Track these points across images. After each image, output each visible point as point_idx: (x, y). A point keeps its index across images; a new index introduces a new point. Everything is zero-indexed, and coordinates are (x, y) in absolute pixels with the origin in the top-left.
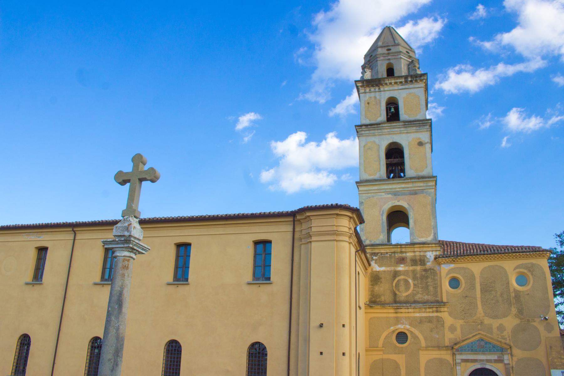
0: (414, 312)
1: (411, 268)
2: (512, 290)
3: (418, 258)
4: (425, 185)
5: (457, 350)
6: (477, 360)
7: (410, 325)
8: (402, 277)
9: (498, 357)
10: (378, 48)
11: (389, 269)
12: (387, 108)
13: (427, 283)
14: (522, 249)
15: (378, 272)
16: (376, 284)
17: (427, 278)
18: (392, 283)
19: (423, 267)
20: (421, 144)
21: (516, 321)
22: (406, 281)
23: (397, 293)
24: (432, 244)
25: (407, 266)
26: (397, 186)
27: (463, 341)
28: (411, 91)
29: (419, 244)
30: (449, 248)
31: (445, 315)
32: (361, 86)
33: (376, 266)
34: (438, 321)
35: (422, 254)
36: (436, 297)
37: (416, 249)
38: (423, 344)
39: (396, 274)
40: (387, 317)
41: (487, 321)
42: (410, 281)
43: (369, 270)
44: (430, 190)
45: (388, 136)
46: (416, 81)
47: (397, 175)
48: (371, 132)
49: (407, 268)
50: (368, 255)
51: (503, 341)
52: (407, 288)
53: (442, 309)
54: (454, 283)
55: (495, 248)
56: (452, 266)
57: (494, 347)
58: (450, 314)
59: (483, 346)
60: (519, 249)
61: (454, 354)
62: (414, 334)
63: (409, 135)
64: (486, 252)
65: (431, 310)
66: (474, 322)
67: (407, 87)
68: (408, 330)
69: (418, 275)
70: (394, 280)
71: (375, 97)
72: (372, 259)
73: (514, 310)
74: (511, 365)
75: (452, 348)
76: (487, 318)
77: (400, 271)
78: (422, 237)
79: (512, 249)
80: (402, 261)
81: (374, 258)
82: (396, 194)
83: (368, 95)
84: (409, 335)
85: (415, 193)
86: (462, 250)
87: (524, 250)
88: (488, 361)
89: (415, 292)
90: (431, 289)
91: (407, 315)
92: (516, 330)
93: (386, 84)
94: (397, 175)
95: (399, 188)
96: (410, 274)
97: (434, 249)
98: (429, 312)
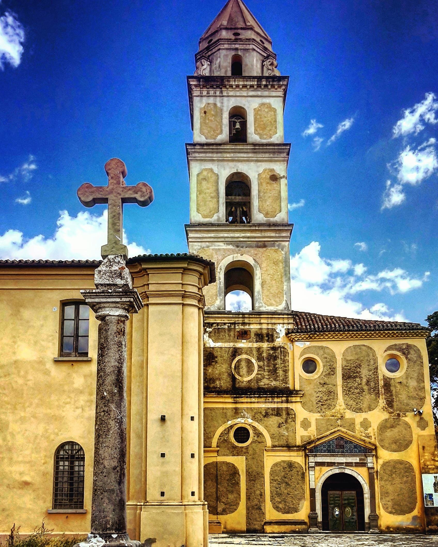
0: (258, 402)
1: (256, 345)
2: (381, 377)
3: (265, 332)
4: (277, 235)
5: (311, 451)
6: (334, 463)
7: (254, 418)
8: (244, 356)
9: (360, 460)
10: (221, 29)
11: (227, 345)
12: (230, 122)
13: (275, 365)
14: (396, 326)
15: (213, 348)
17: (275, 358)
19: (271, 345)
20: (274, 178)
21: (385, 416)
22: (249, 362)
23: (237, 376)
24: (283, 315)
32: (196, 86)
33: (210, 340)
34: (288, 414)
35: (270, 327)
36: (286, 383)
37: (263, 321)
38: (269, 442)
39: (235, 352)
40: (223, 408)
41: (349, 415)
42: (254, 361)
44: (283, 243)
45: (231, 164)
46: (273, 86)
47: (238, 219)
48: (208, 155)
49: (250, 345)
51: (366, 439)
53: (294, 399)
54: (309, 365)
56: (308, 344)
57: (356, 447)
59: (341, 445)
60: (392, 326)
61: (306, 456)
63: (260, 163)
65: (279, 400)
67: (259, 93)
68: (250, 425)
69: (265, 355)
71: (215, 105)
73: (382, 402)
74: (375, 469)
75: (305, 449)
78: (271, 305)
80: (244, 335)
81: (208, 329)
82: (238, 244)
83: (205, 100)
84: (251, 432)
85: (264, 245)
87: (398, 327)
88: (349, 464)
89: (259, 376)
90: (280, 372)
91: (249, 406)
92: (383, 427)
94: (238, 219)
95: (243, 237)
96: (255, 353)
97: (286, 321)
98: (278, 402)
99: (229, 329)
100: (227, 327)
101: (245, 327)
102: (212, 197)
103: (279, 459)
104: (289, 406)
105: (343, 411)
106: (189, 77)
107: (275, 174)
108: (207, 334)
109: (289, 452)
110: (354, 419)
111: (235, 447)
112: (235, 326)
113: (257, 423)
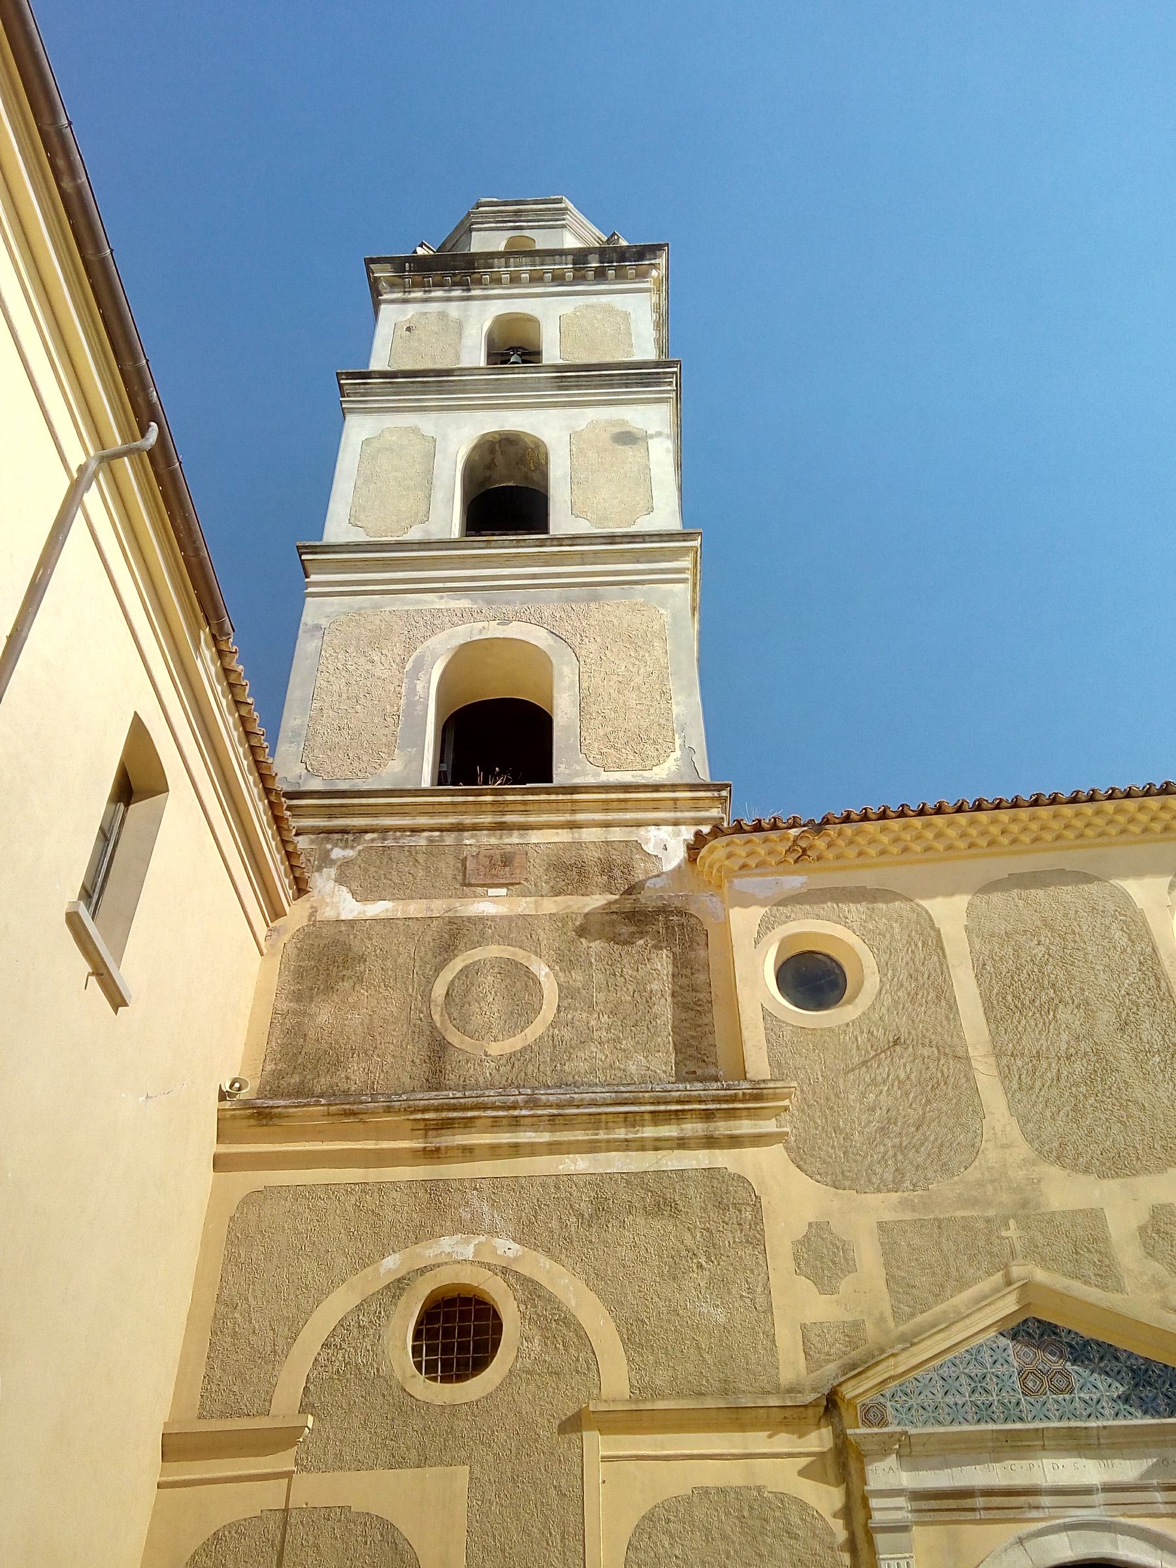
7: (526, 1234)
11: (415, 908)
15: (352, 923)
16: (329, 989)
18: (430, 983)
20: (627, 438)
22: (518, 979)
23: (454, 1037)
25: (525, 894)
27: (910, 1341)
28: (593, 299)
31: (764, 1166)
35: (616, 834)
38: (615, 1379)
39: (455, 935)
41: (1064, 1192)
42: (541, 970)
43: (296, 913)
49: (525, 905)
52: (523, 1004)
54: (813, 979)
58: (800, 1158)
62: (551, 1299)
66: (974, 1202)
68: (505, 1271)
70: (439, 968)
72: (325, 860)
76: (1054, 1171)
77: (482, 920)
80: (501, 869)
81: (337, 853)
89: (567, 1034)
93: (497, 281)
99: (433, 848)
100: (423, 842)
101: (507, 841)
102: (408, 488)
103: (680, 1480)
104: (721, 1158)
105: (1022, 1173)
106: (369, 261)
107: (628, 429)
108: (332, 872)
109: (738, 1435)
110: (1095, 1216)
111: (405, 1404)
113: (545, 1262)
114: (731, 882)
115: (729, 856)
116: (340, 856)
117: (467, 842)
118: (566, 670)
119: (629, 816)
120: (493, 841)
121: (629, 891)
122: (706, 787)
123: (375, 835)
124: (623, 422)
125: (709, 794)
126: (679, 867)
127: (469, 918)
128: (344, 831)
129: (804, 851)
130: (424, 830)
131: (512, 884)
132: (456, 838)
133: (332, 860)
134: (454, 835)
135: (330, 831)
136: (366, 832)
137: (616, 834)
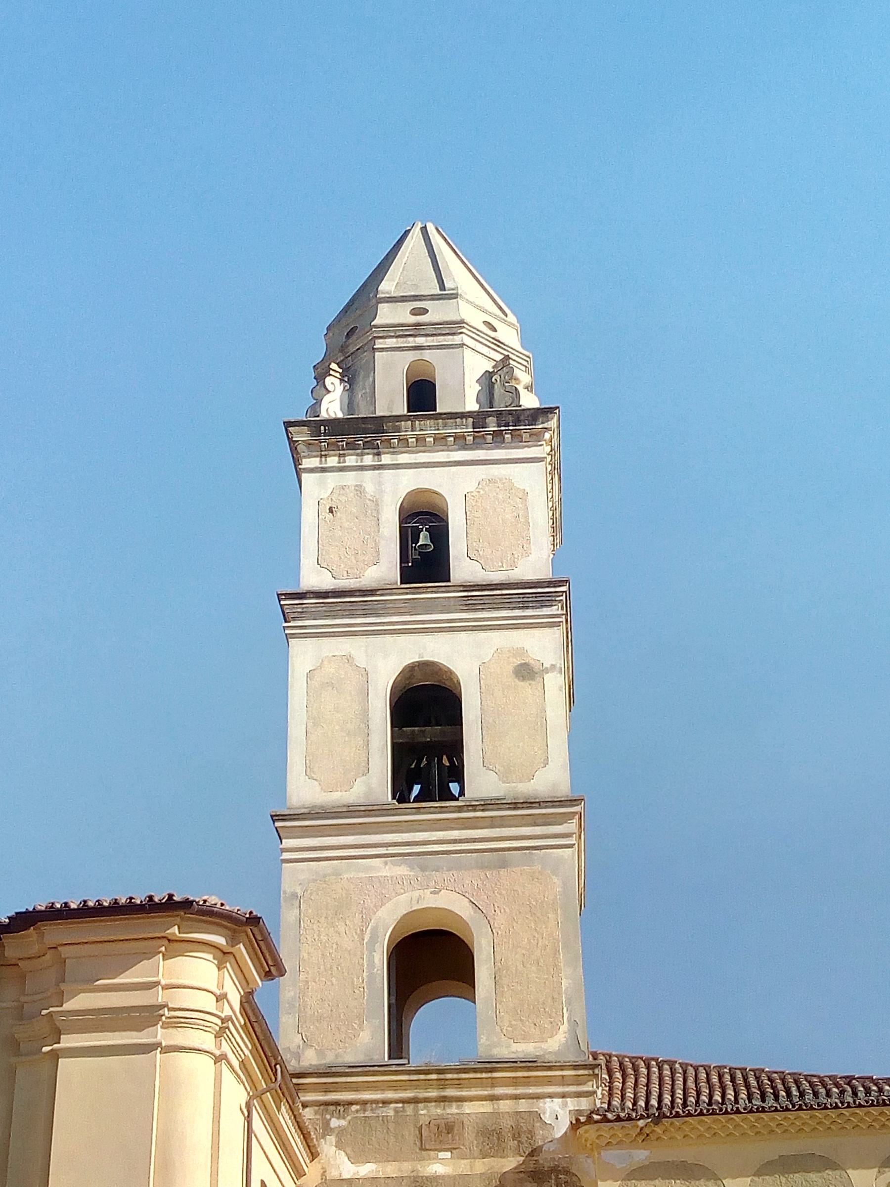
3: (507, 1123)
11: (391, 1169)
24: (562, 1068)
26: (430, 828)
29: (514, 1064)
30: (630, 1082)
35: (523, 1106)
49: (463, 1167)
50: (308, 1114)
55: (805, 1085)
64: (770, 1102)
72: (327, 1129)
78: (526, 1038)
79: (868, 1091)
80: (445, 1134)
81: (335, 1123)
86: (679, 1093)
100: (392, 1113)
101: (449, 1111)
112: (416, 1111)
114: (599, 1154)
115: (598, 1137)
116: (336, 1125)
117: (422, 1112)
118: (484, 942)
119: (532, 1090)
120: (439, 1111)
121: (532, 1154)
122: (585, 1067)
123: (358, 1107)
124: (521, 652)
125: (586, 1072)
126: (566, 1133)
127: (427, 1177)
128: (337, 1103)
129: (648, 1135)
130: (391, 1103)
131: (455, 1149)
132: (414, 1109)
133: (331, 1129)
134: (412, 1106)
135: (327, 1104)
136: (352, 1104)
137: (523, 1106)
